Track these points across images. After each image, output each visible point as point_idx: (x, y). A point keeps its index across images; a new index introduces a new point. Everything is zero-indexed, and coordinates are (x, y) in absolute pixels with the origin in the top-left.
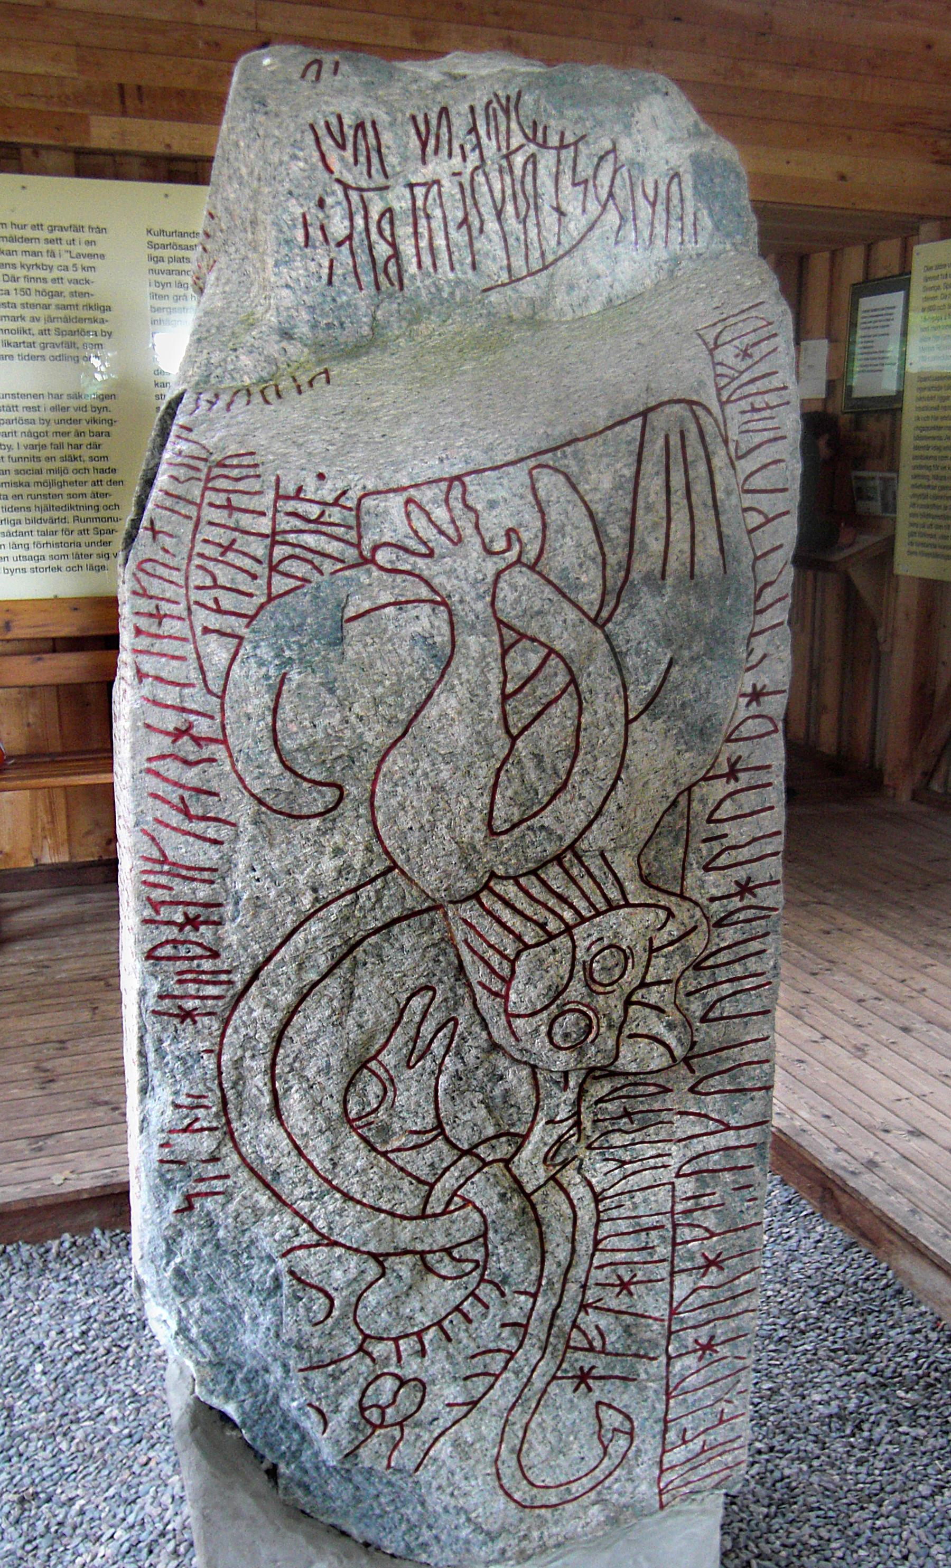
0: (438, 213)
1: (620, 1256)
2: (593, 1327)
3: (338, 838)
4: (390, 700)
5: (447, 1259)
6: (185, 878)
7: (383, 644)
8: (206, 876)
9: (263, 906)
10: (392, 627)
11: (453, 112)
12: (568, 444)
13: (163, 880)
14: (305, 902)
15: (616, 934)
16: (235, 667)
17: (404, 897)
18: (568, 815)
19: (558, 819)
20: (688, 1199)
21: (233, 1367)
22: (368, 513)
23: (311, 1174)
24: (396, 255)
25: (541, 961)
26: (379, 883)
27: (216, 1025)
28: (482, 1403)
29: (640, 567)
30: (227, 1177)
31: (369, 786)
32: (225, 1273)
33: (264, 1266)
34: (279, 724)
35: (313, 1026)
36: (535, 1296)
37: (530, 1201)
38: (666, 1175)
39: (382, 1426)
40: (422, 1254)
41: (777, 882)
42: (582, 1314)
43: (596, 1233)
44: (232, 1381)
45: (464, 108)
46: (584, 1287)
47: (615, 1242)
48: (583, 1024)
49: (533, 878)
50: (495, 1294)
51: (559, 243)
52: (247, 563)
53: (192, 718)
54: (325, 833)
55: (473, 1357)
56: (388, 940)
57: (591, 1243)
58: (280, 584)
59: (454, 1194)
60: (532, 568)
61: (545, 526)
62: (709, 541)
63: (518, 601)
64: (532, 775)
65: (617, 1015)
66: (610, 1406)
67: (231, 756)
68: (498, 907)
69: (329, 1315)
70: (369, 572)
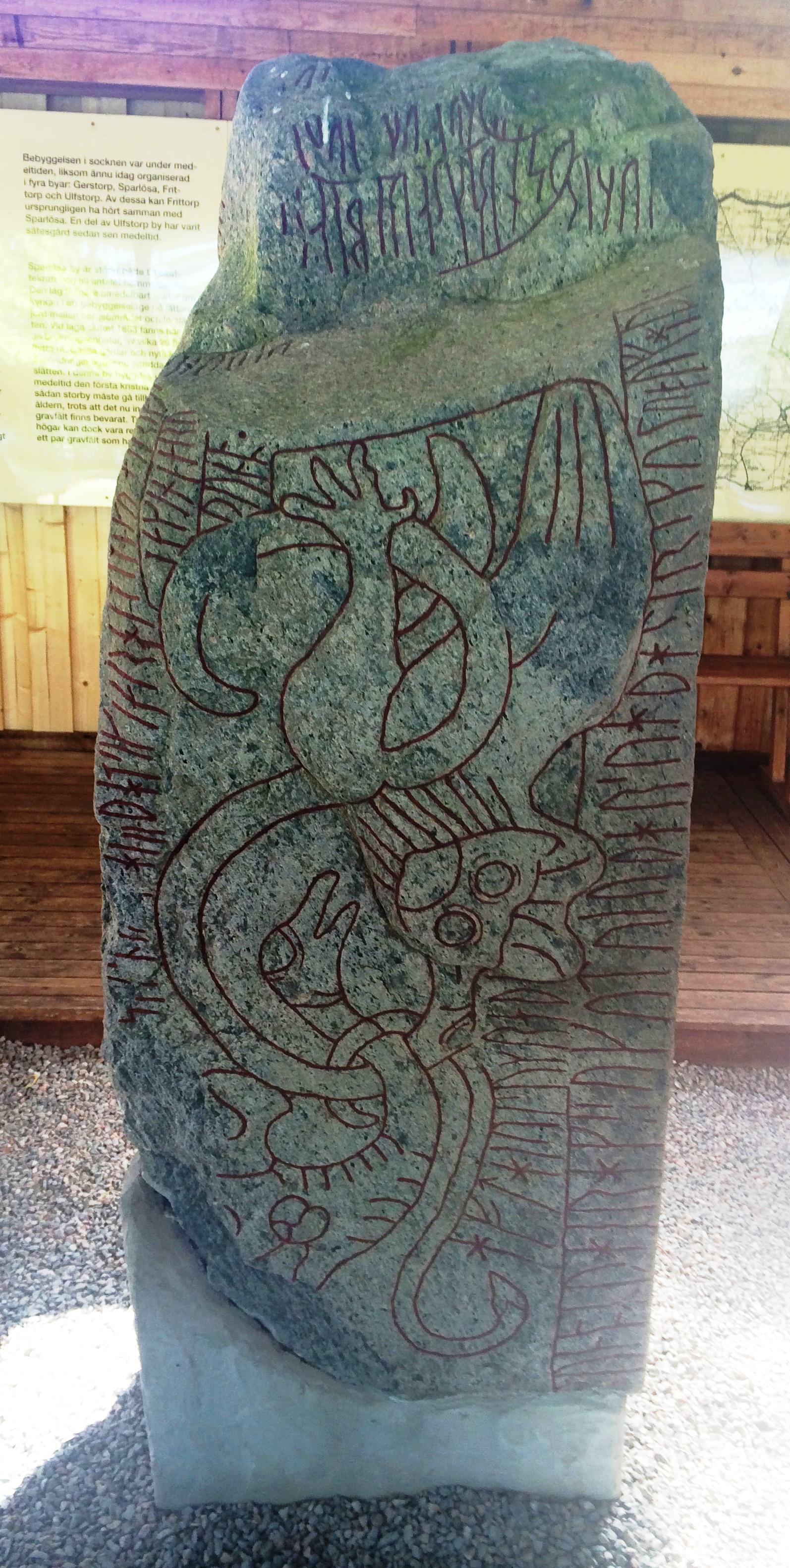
0: (401, 203)
1: (514, 1143)
3: (253, 736)
5: (349, 1109)
6: (130, 753)
8: (145, 752)
9: (191, 784)
11: (420, 110)
12: (466, 416)
13: (114, 752)
15: (502, 853)
16: (169, 587)
18: (455, 744)
19: (444, 744)
20: (583, 1106)
22: (279, 467)
23: (230, 1013)
24: (363, 241)
25: (428, 865)
26: (288, 778)
27: (153, 875)
28: (380, 1244)
29: (528, 529)
30: (162, 1000)
33: (191, 1080)
35: (232, 888)
36: (431, 1160)
37: (428, 1075)
39: (288, 1241)
40: (327, 1100)
41: (683, 830)
42: (478, 1188)
43: (493, 1117)
44: (170, 1172)
45: (431, 107)
46: (480, 1163)
48: (466, 926)
50: (393, 1149)
51: (514, 229)
52: (179, 502)
53: (138, 624)
54: (242, 729)
57: (487, 1125)
58: (207, 522)
59: (356, 1053)
60: (425, 523)
61: (439, 487)
63: (410, 551)
64: (421, 702)
65: (501, 923)
66: (503, 1279)
69: (242, 1132)
70: (278, 517)
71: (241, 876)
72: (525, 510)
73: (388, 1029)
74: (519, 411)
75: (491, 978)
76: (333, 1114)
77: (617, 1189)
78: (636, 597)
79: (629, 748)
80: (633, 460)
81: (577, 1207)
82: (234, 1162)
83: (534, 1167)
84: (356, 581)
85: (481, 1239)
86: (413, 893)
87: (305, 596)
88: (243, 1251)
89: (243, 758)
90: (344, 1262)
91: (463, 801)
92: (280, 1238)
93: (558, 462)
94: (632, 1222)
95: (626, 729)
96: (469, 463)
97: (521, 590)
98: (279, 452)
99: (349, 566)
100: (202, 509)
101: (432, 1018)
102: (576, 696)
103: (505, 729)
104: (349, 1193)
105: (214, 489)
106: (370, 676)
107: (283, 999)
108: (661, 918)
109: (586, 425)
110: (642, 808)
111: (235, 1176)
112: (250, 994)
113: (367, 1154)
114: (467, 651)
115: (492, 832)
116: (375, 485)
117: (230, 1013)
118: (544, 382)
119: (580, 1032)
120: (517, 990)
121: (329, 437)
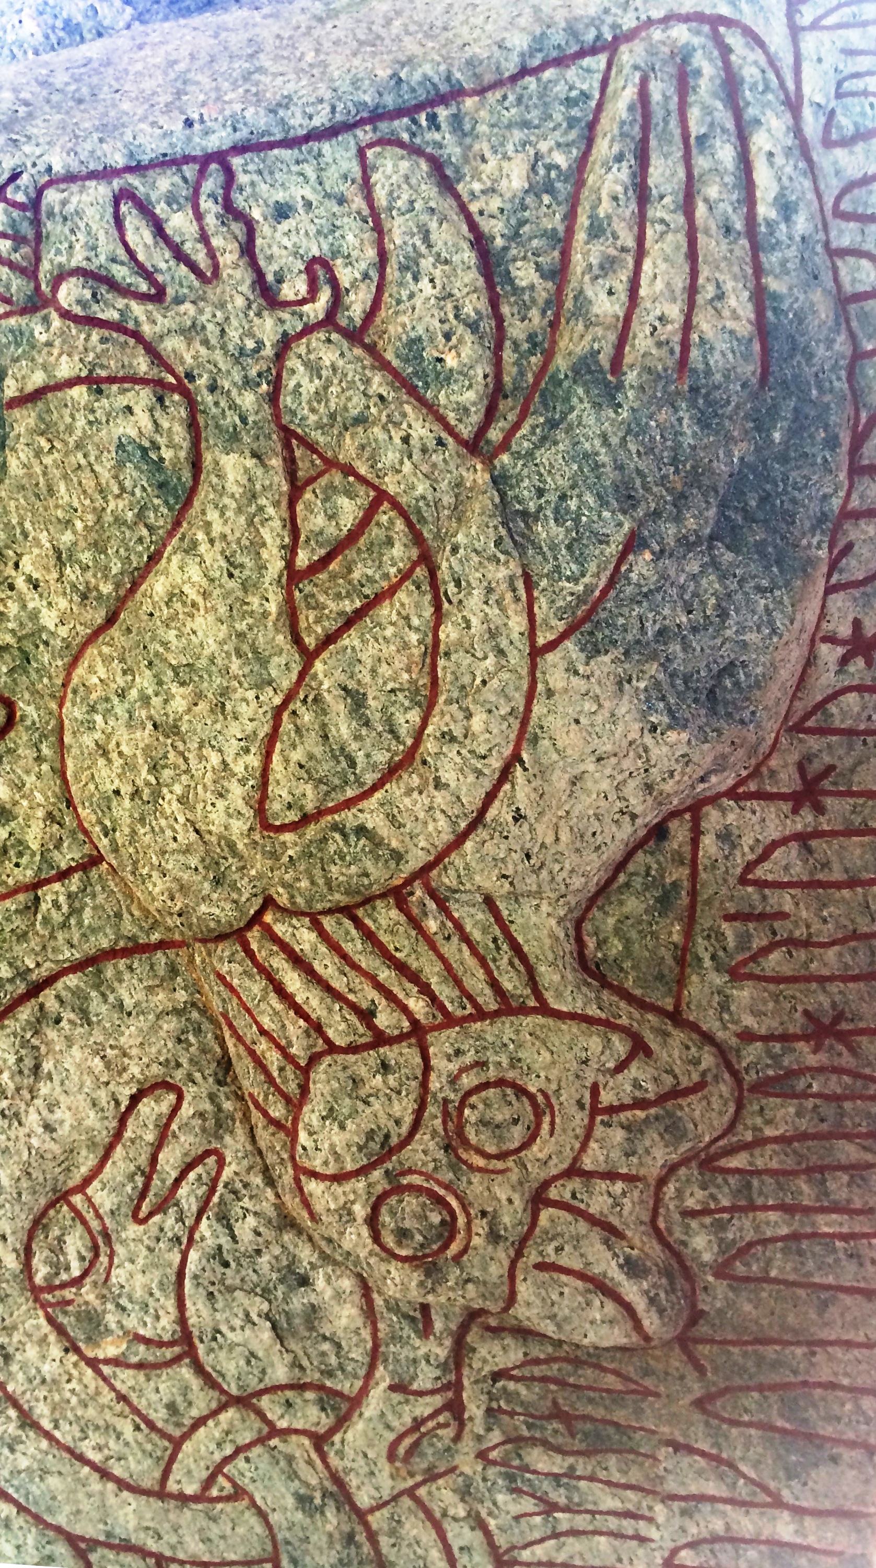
17: (118, 915)
18: (415, 817)
19: (392, 819)
25: (356, 1082)
26: (75, 882)
29: (573, 344)
31: (54, 706)
48: (435, 1218)
49: (347, 923)
56: (97, 987)
59: (218, 1470)
60: (354, 336)
61: (383, 257)
63: (320, 396)
65: (511, 1217)
68: (279, 963)
72: (569, 304)
73: (283, 1424)
74: (560, 89)
75: (496, 1331)
86: (326, 1139)
91: (433, 946)
95: (786, 807)
97: (556, 483)
99: (193, 426)
102: (677, 723)
103: (521, 789)
106: (235, 666)
107: (72, 1347)
110: (822, 980)
114: (439, 616)
115: (496, 1014)
118: (614, 26)
119: (686, 1460)
120: (549, 1360)
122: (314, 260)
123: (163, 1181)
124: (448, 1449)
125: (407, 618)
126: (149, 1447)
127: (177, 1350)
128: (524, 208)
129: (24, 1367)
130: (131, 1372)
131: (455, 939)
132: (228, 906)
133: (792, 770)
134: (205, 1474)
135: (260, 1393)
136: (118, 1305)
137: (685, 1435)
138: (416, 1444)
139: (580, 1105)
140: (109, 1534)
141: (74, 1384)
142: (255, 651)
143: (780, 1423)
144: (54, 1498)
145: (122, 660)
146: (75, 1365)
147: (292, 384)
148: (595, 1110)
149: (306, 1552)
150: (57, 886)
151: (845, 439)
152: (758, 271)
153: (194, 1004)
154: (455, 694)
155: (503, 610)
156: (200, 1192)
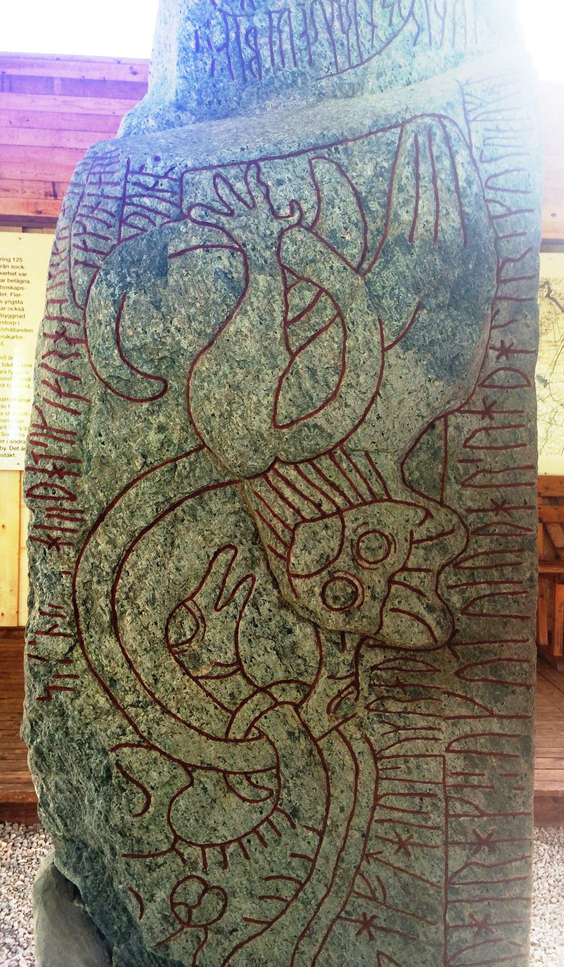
1: (397, 815)
2: (374, 878)
3: (162, 419)
4: (201, 318)
5: (245, 783)
6: (55, 438)
7: (194, 276)
8: (69, 437)
9: (107, 464)
10: (200, 263)
12: (341, 143)
14: (137, 464)
15: (379, 522)
16: (93, 287)
17: (211, 471)
18: (336, 420)
19: (328, 420)
20: (458, 774)
21: (81, 845)
22: (187, 183)
25: (315, 533)
26: (192, 457)
27: (72, 554)
28: (275, 925)
29: (394, 231)
30: (76, 677)
31: (185, 381)
32: (71, 758)
34: (121, 329)
36: (321, 834)
37: (317, 746)
38: (438, 748)
39: (188, 924)
40: (226, 773)
41: (532, 508)
42: (364, 863)
43: (376, 789)
44: (80, 857)
46: (365, 836)
47: (393, 801)
48: (349, 590)
50: (286, 824)
52: (104, 216)
53: (66, 324)
54: (153, 413)
55: (268, 879)
56: (200, 504)
57: (372, 797)
58: (126, 232)
59: (252, 725)
60: (309, 229)
62: (452, 216)
63: (296, 252)
64: (307, 384)
65: (380, 589)
66: (391, 960)
67: (89, 351)
68: (282, 485)
69: (146, 809)
70: (186, 224)
71: (151, 552)
72: (392, 217)
73: (281, 700)
74: (384, 140)
75: (372, 647)
76: (231, 789)
77: (493, 859)
78: (485, 295)
79: (483, 432)
80: (477, 179)
81: (456, 880)
82: (139, 841)
83: (415, 839)
84: (252, 277)
85: (368, 918)
86: (302, 559)
87: (208, 291)
88: (146, 936)
89: (153, 437)
90: (240, 946)
91: (345, 475)
92: (181, 921)
93: (417, 177)
94: (507, 895)
95: (480, 416)
96: (344, 179)
98: (186, 171)
100: (122, 221)
101: (320, 688)
102: (438, 378)
104: (245, 872)
105: (133, 204)
106: (263, 360)
108: (518, 588)
109: (440, 147)
110: (497, 486)
111: (139, 856)
112: (157, 667)
113: (262, 829)
114: (346, 337)
115: (371, 503)
116: (267, 196)
117: (138, 687)
118: (402, 118)
119: (453, 699)
120: (395, 659)
121: (228, 157)
122: (293, 201)
123: (228, 591)
124: (353, 705)
125: (333, 338)
126: (221, 717)
127: (235, 667)
128: (373, 182)
129: (164, 684)
130: (214, 681)
131: (354, 471)
132: (260, 461)
133: (481, 401)
134: (246, 728)
135: (270, 686)
136: (208, 650)
137: (452, 688)
138: (339, 704)
139: (406, 541)
140: (202, 762)
141: (187, 690)
142: (271, 354)
143: (490, 678)
144: (178, 745)
145: (215, 360)
146: (188, 681)
147: (285, 247)
148: (412, 542)
149: (292, 760)
150: (185, 459)
151: (495, 268)
152: (461, 205)
153: (243, 509)
154: (353, 368)
155: (371, 333)
156: (245, 594)
